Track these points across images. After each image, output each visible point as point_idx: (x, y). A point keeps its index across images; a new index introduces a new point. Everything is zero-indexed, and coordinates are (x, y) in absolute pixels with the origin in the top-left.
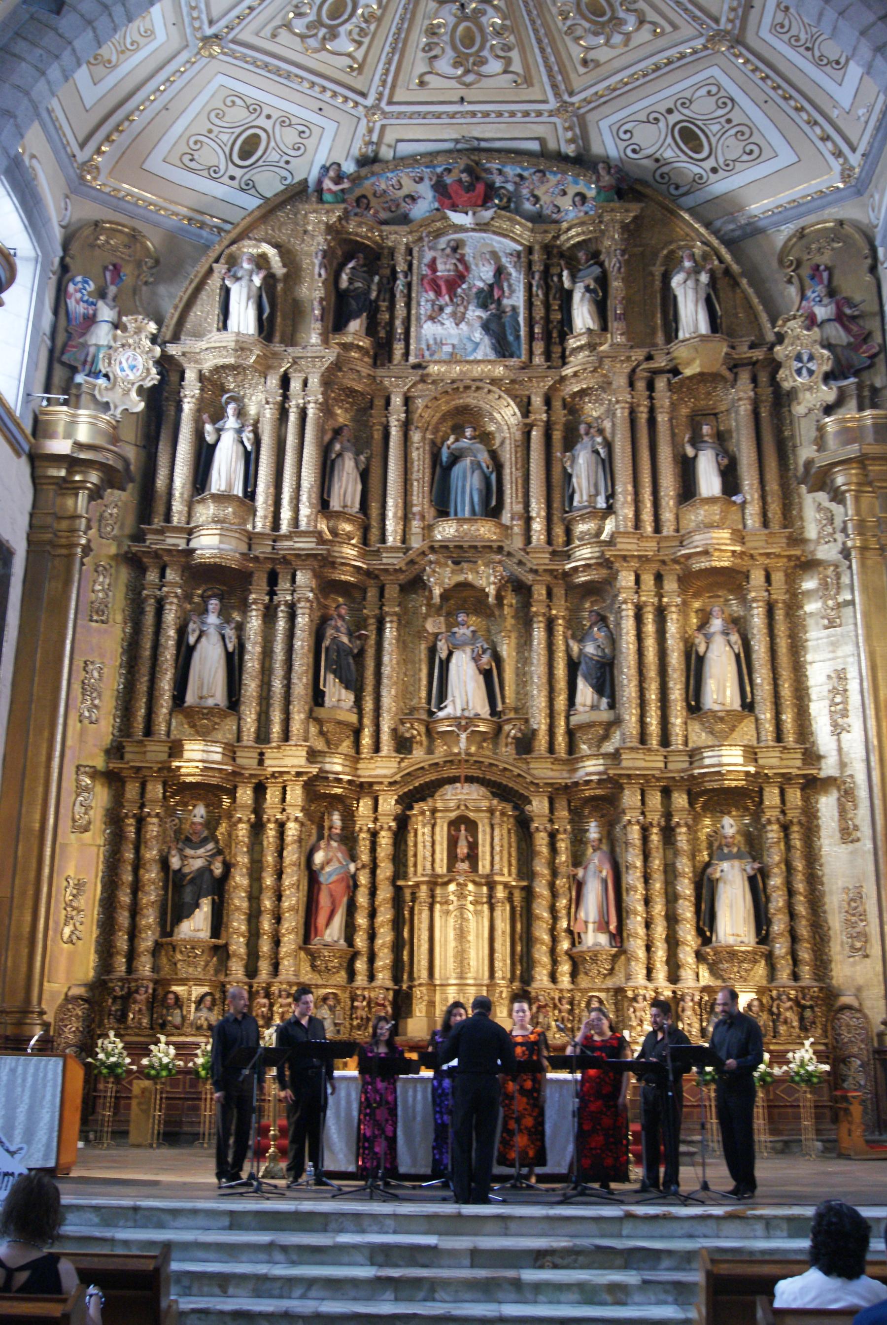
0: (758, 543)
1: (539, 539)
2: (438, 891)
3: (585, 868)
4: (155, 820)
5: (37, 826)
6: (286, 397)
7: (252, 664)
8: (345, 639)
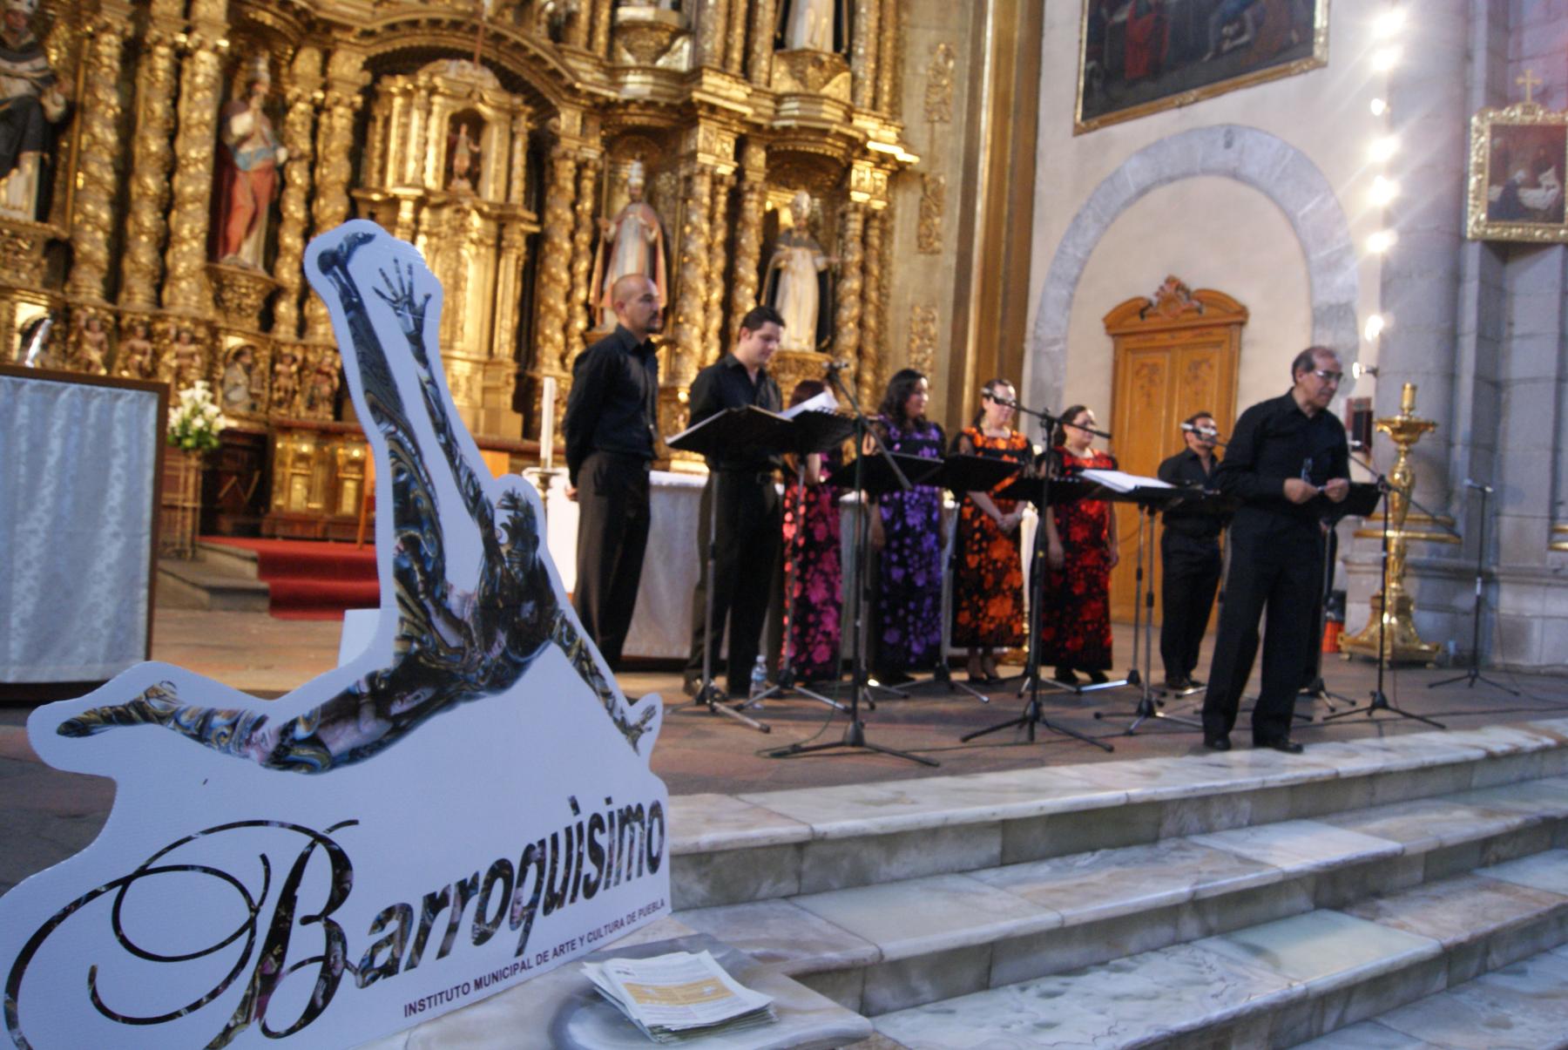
2: (425, 214)
3: (619, 223)
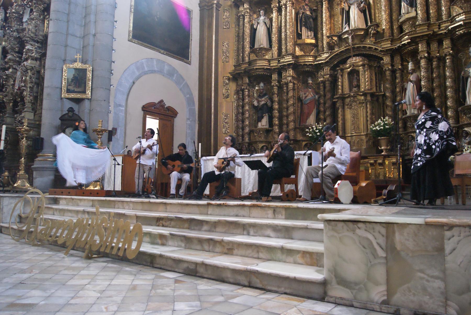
5: (209, 97)
7: (274, 30)
8: (308, 13)
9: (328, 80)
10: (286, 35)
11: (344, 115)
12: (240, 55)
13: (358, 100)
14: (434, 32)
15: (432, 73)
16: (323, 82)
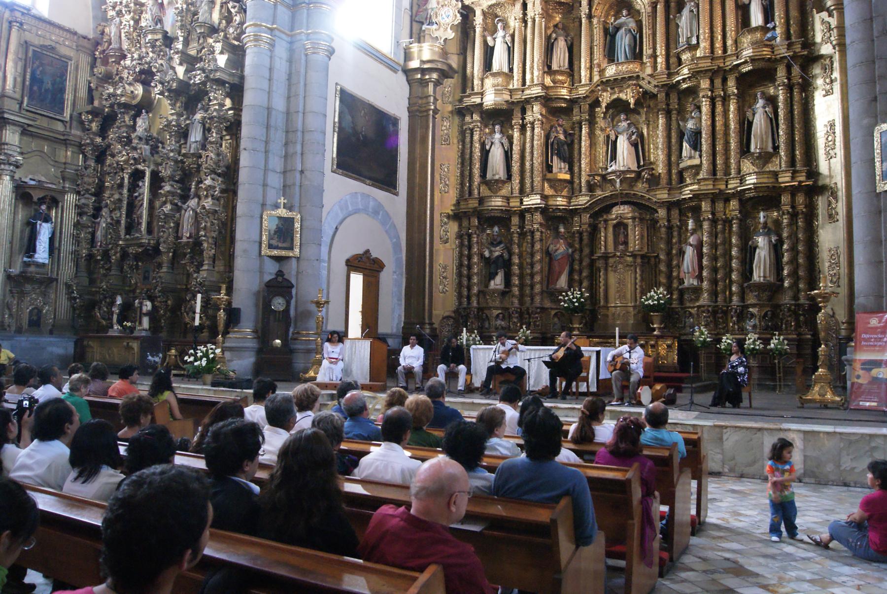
0: (782, 51)
1: (661, 67)
4: (475, 236)
6: (525, 14)
7: (516, 156)
8: (562, 137)
9: (587, 231)
10: (532, 165)
11: (606, 280)
12: (465, 185)
13: (626, 261)
14: (720, 190)
15: (716, 238)
16: (580, 233)
